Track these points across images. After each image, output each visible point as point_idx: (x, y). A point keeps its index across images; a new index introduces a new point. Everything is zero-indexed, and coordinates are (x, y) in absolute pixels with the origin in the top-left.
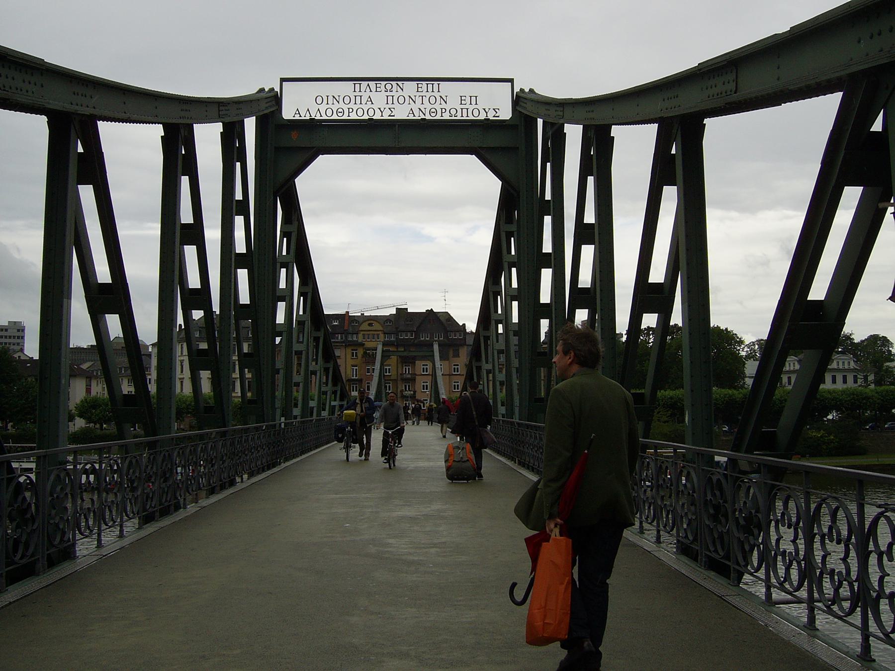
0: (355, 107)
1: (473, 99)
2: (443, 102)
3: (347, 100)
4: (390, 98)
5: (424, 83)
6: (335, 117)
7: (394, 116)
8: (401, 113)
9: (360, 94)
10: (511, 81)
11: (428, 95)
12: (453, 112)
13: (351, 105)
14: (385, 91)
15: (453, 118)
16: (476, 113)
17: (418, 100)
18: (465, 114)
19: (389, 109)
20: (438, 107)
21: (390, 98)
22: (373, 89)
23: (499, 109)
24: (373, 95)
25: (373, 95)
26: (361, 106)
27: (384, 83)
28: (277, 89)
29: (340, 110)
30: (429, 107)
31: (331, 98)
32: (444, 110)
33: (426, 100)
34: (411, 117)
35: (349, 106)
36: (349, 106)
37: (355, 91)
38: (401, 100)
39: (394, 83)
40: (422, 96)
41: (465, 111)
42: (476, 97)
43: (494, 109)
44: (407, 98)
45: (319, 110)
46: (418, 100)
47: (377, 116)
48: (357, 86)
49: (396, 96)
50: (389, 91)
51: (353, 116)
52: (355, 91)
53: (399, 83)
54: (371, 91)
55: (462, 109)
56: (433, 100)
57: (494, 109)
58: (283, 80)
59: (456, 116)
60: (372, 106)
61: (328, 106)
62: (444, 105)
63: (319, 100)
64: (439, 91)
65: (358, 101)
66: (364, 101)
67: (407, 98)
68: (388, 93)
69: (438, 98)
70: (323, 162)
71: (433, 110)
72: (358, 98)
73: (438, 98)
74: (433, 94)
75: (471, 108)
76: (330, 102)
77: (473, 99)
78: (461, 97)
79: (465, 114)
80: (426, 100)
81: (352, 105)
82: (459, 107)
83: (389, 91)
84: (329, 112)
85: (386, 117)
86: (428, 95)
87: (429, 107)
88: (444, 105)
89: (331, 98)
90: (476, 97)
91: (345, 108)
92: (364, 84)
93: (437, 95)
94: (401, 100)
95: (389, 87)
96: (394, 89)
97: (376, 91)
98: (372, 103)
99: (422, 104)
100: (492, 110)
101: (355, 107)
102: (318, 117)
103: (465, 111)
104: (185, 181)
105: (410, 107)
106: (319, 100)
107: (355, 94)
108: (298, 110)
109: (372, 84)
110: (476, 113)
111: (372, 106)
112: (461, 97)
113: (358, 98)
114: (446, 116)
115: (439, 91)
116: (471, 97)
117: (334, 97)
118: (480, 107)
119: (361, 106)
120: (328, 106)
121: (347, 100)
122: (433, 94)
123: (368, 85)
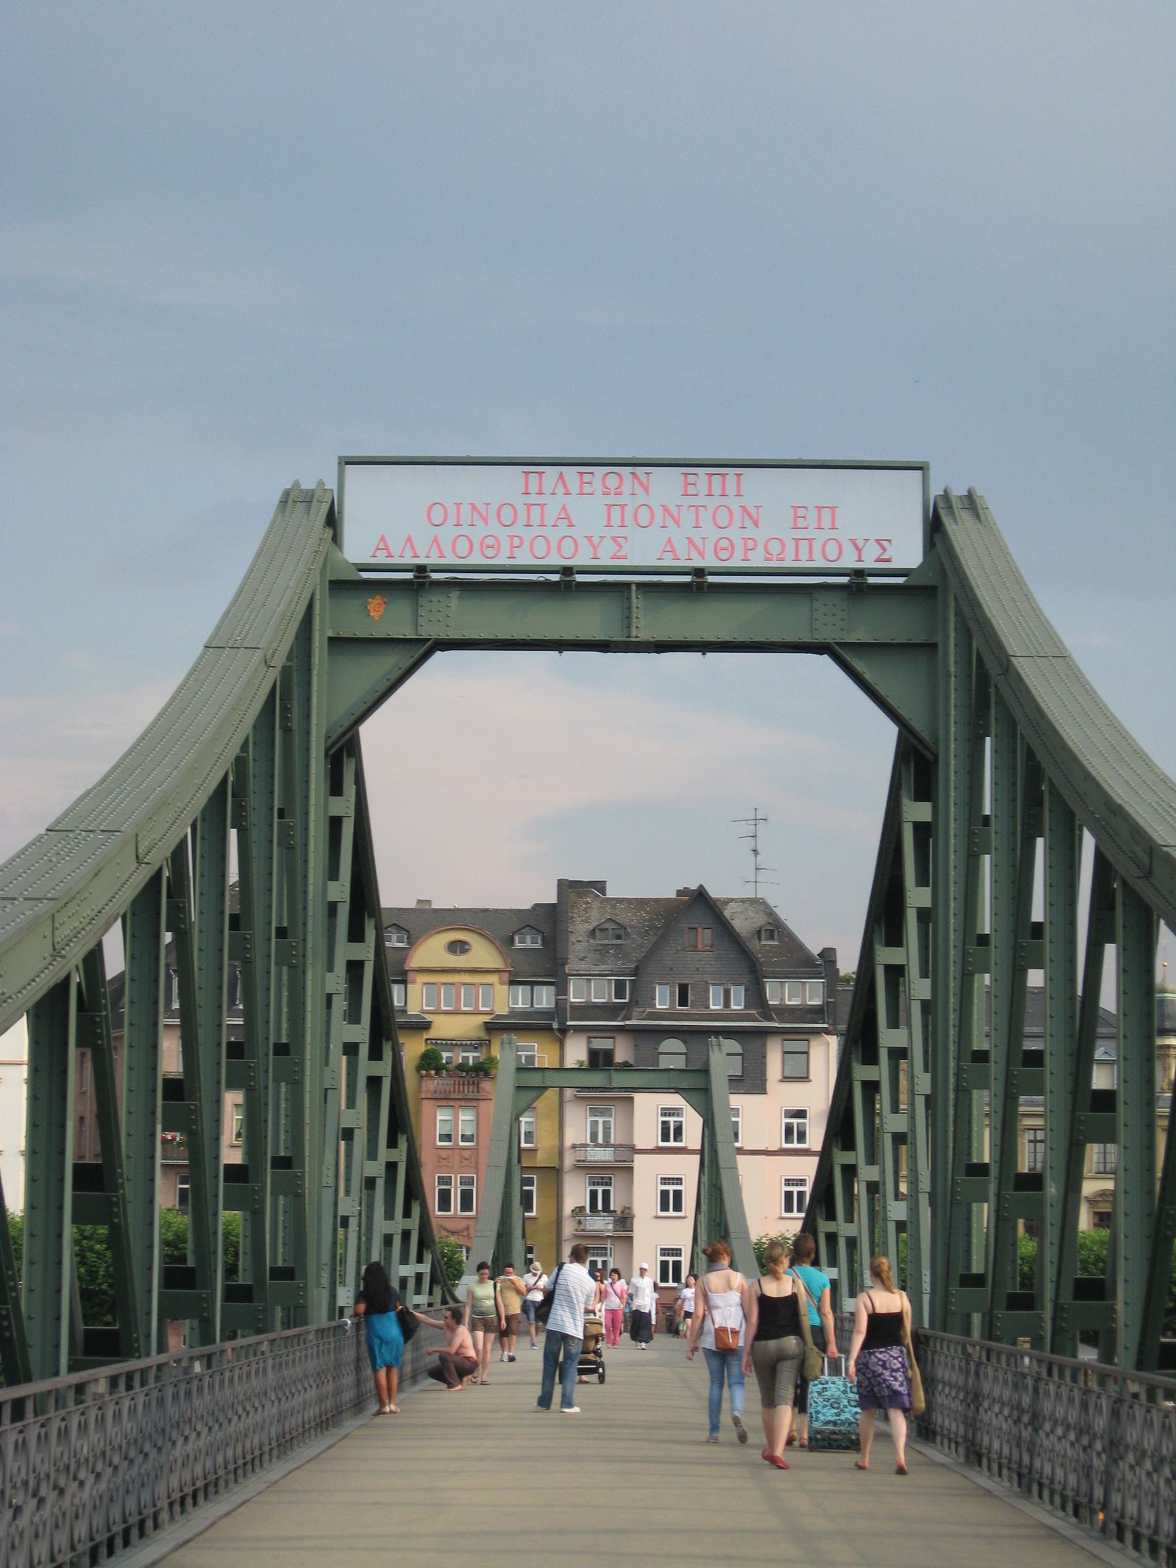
1: (826, 514)
3: (507, 514)
4: (616, 512)
11: (712, 503)
12: (774, 548)
14: (605, 494)
17: (687, 517)
18: (804, 555)
19: (614, 539)
20: (735, 534)
21: (616, 512)
23: (889, 541)
24: (575, 504)
29: (490, 541)
30: (713, 534)
32: (750, 544)
33: (706, 517)
38: (644, 518)
42: (833, 509)
43: (878, 541)
45: (435, 540)
46: (687, 517)
54: (568, 493)
56: (723, 518)
57: (878, 541)
59: (782, 559)
65: (535, 520)
66: (550, 519)
67: (659, 512)
68: (611, 499)
71: (724, 543)
73: (737, 512)
74: (724, 500)
75: (820, 537)
76: (465, 518)
77: (826, 514)
78: (795, 508)
79: (804, 555)
80: (706, 517)
82: (788, 536)
87: (713, 534)
88: (751, 531)
89: (466, 510)
90: (833, 509)
91: (503, 534)
93: (733, 503)
94: (644, 518)
95: (612, 482)
96: (627, 488)
109: (570, 472)
113: (535, 511)
117: (473, 507)
123: (561, 476)
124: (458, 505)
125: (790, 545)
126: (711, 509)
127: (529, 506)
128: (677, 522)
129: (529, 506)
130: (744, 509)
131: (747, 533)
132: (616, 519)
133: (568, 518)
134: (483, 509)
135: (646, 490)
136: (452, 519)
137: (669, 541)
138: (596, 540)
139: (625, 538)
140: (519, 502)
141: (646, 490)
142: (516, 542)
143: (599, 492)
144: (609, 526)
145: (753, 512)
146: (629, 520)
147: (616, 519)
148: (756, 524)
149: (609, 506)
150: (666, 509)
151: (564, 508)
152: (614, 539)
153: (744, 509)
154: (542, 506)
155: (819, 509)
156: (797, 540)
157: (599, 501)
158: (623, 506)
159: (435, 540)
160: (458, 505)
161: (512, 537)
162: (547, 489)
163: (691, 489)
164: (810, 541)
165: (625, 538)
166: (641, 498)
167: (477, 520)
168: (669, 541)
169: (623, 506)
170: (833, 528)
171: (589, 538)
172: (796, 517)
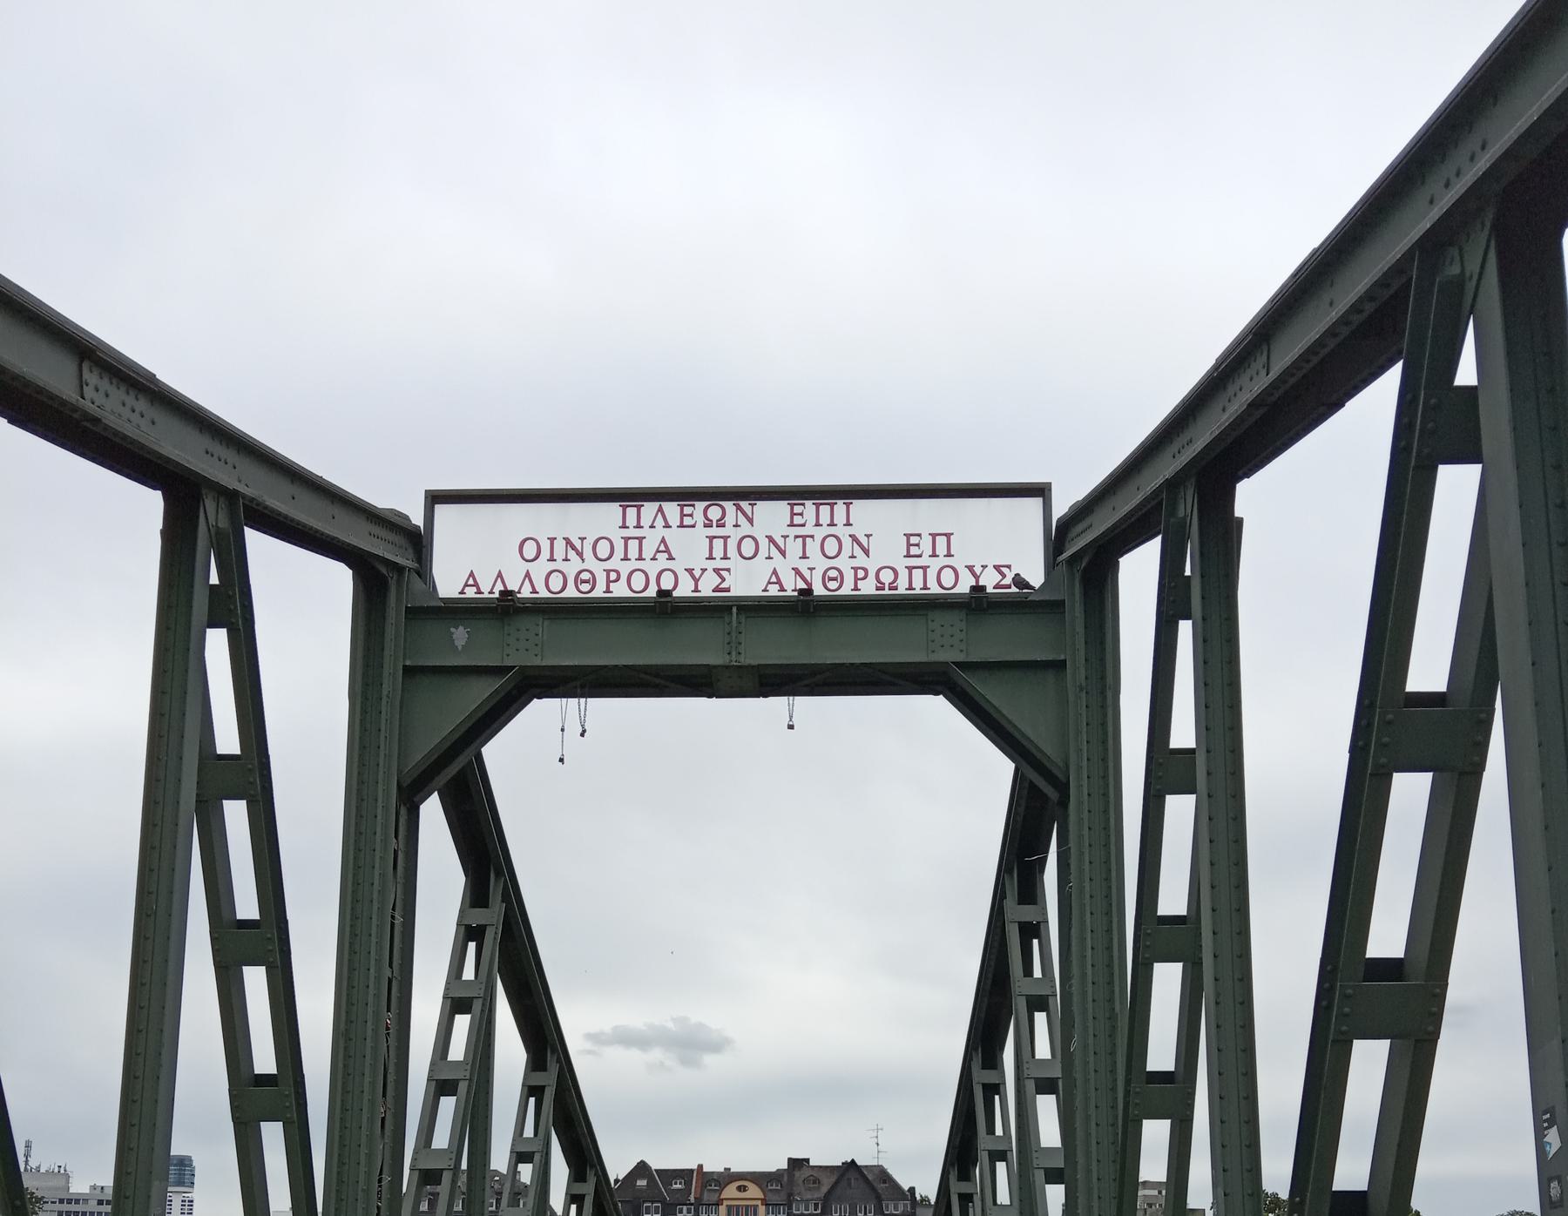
0: (625, 569)
1: (941, 541)
2: (858, 551)
3: (603, 548)
4: (718, 544)
5: (809, 503)
6: (571, 592)
7: (728, 590)
8: (748, 582)
9: (638, 533)
10: (1041, 491)
13: (615, 563)
15: (887, 592)
16: (948, 578)
17: (794, 548)
19: (717, 571)
20: (844, 563)
21: (718, 544)
22: (674, 518)
24: (675, 537)
25: (675, 537)
26: (640, 565)
27: (700, 505)
28: (418, 519)
29: (585, 576)
30: (821, 564)
31: (560, 546)
33: (813, 547)
34: (774, 591)
35: (609, 565)
36: (609, 565)
37: (624, 526)
38: (748, 547)
39: (729, 506)
40: (804, 537)
41: (918, 574)
43: (997, 568)
44: (764, 543)
45: (528, 575)
46: (794, 548)
47: (684, 590)
48: (632, 512)
49: (735, 535)
50: (714, 524)
51: (620, 591)
52: (624, 526)
53: (744, 504)
54: (667, 526)
55: (910, 569)
57: (997, 568)
58: (435, 498)
60: (669, 565)
61: (552, 566)
62: (861, 560)
63: (530, 549)
64: (848, 524)
66: (647, 554)
67: (764, 543)
68: (714, 531)
69: (847, 542)
70: (541, 713)
71: (833, 573)
72: (633, 545)
73: (847, 542)
74: (832, 530)
75: (935, 565)
76: (559, 554)
77: (941, 541)
78: (908, 536)
81: (615, 563)
82: (901, 564)
83: (714, 524)
84: (556, 582)
85: (706, 590)
86: (820, 533)
87: (821, 564)
88: (861, 560)
89: (560, 546)
90: (948, 536)
91: (599, 569)
92: (649, 508)
93: (840, 530)
94: (748, 547)
95: (714, 513)
97: (682, 526)
98: (671, 558)
99: (804, 557)
100: (990, 569)
101: (625, 569)
102: (526, 593)
103: (918, 574)
104: (217, 643)
105: (770, 565)
106: (530, 549)
107: (626, 533)
108: (472, 575)
109: (672, 509)
110: (948, 578)
111: (669, 565)
112: (908, 536)
113: (633, 545)
114: (868, 588)
115: (848, 524)
116: (934, 536)
118: (959, 562)
119: (640, 565)
120: (552, 566)
121: (603, 548)
122: (832, 530)
123: (660, 509)
124: (552, 540)
125: (903, 575)
126: (818, 539)
127: (626, 539)
128: (783, 553)
129: (626, 539)
130: (854, 538)
131: (855, 563)
132: (718, 551)
133: (667, 551)
134: (578, 544)
135: (751, 521)
136: (545, 554)
137: (775, 572)
138: (697, 573)
139: (728, 570)
140: (617, 536)
141: (751, 521)
142: (613, 576)
143: (700, 525)
144: (711, 558)
145: (864, 541)
146: (732, 551)
147: (718, 551)
148: (867, 552)
149: (711, 538)
150: (771, 540)
151: (663, 541)
152: (717, 571)
153: (854, 538)
154: (640, 539)
155: (934, 536)
156: (910, 569)
157: (701, 532)
158: (726, 538)
159: (528, 575)
160: (552, 540)
161: (608, 572)
162: (645, 522)
163: (797, 520)
164: (925, 568)
165: (728, 570)
166: (746, 528)
167: (572, 554)
168: (775, 572)
169: (726, 538)
170: (949, 555)
171: (690, 571)
172: (909, 545)
